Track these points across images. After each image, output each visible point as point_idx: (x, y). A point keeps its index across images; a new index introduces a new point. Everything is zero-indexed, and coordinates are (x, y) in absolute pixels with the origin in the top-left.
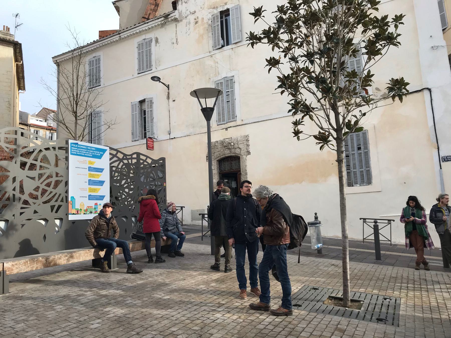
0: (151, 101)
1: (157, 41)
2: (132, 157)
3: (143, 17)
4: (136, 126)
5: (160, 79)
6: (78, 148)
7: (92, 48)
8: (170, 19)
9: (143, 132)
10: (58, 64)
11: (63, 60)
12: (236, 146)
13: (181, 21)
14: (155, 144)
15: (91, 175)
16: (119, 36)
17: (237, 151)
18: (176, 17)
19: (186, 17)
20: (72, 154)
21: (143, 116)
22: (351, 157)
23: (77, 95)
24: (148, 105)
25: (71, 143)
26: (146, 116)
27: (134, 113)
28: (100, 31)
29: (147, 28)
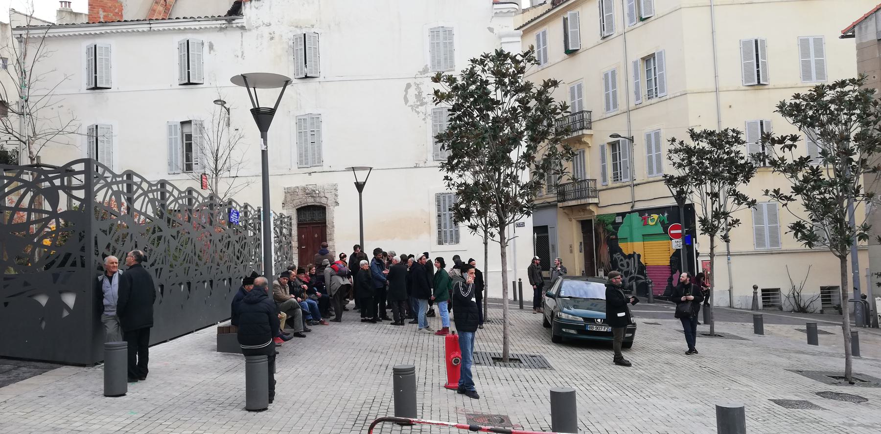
1: (211, 47)
8: (234, 26)
12: (322, 194)
13: (250, 30)
17: (324, 201)
18: (244, 25)
19: (257, 27)
22: (442, 217)
24: (196, 130)
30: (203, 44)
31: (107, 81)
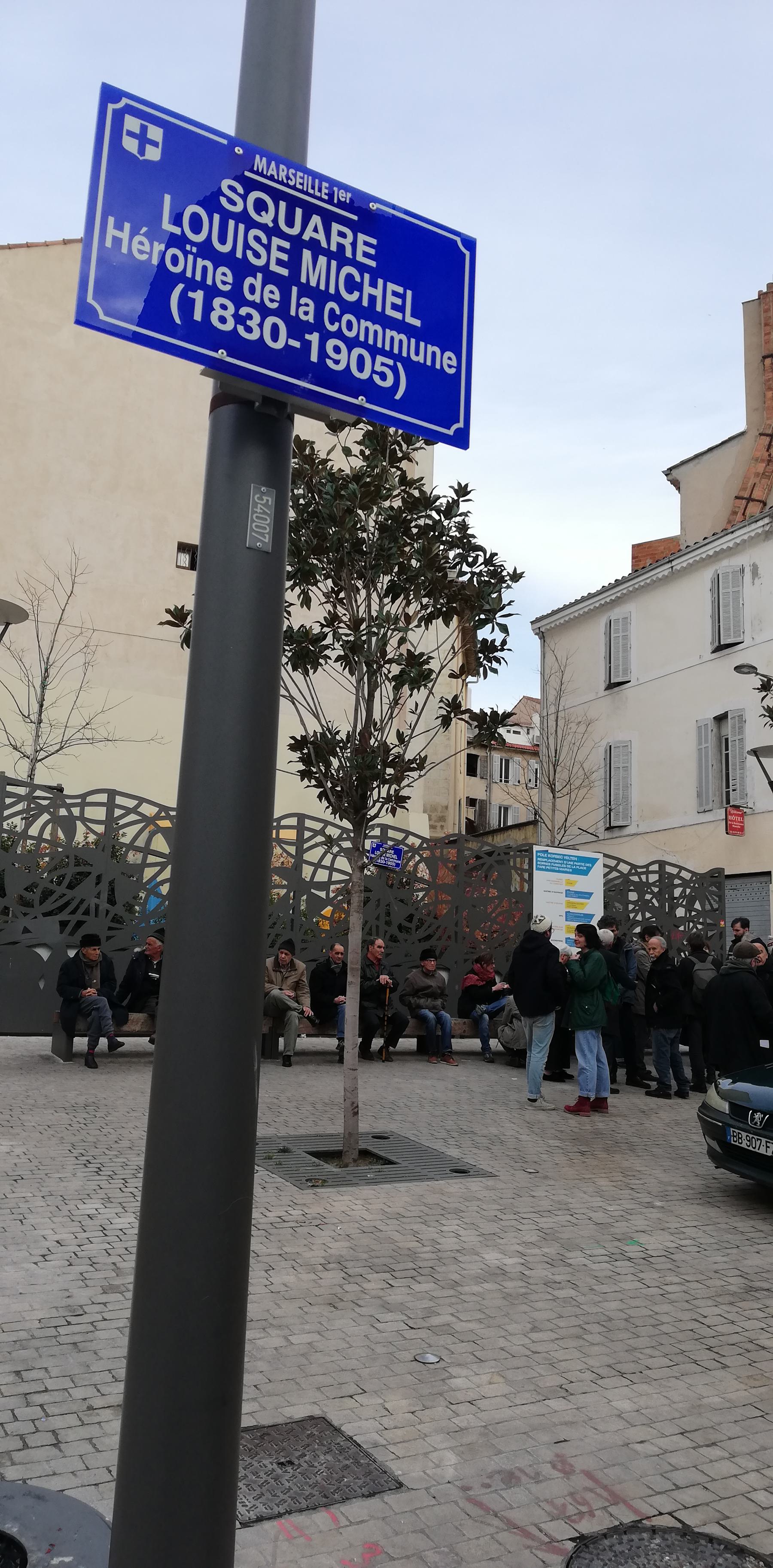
0: (741, 716)
2: (648, 869)
3: (737, 498)
4: (707, 776)
5: (756, 669)
6: (548, 858)
7: (613, 597)
9: (724, 790)
10: (542, 635)
11: (553, 625)
14: (748, 822)
15: (569, 904)
16: (669, 565)
20: (538, 869)
21: (724, 752)
23: (556, 750)
24: (733, 727)
25: (537, 852)
26: (729, 751)
27: (704, 746)
28: (634, 546)
29: (731, 544)
30: (742, 570)
31: (626, 671)
